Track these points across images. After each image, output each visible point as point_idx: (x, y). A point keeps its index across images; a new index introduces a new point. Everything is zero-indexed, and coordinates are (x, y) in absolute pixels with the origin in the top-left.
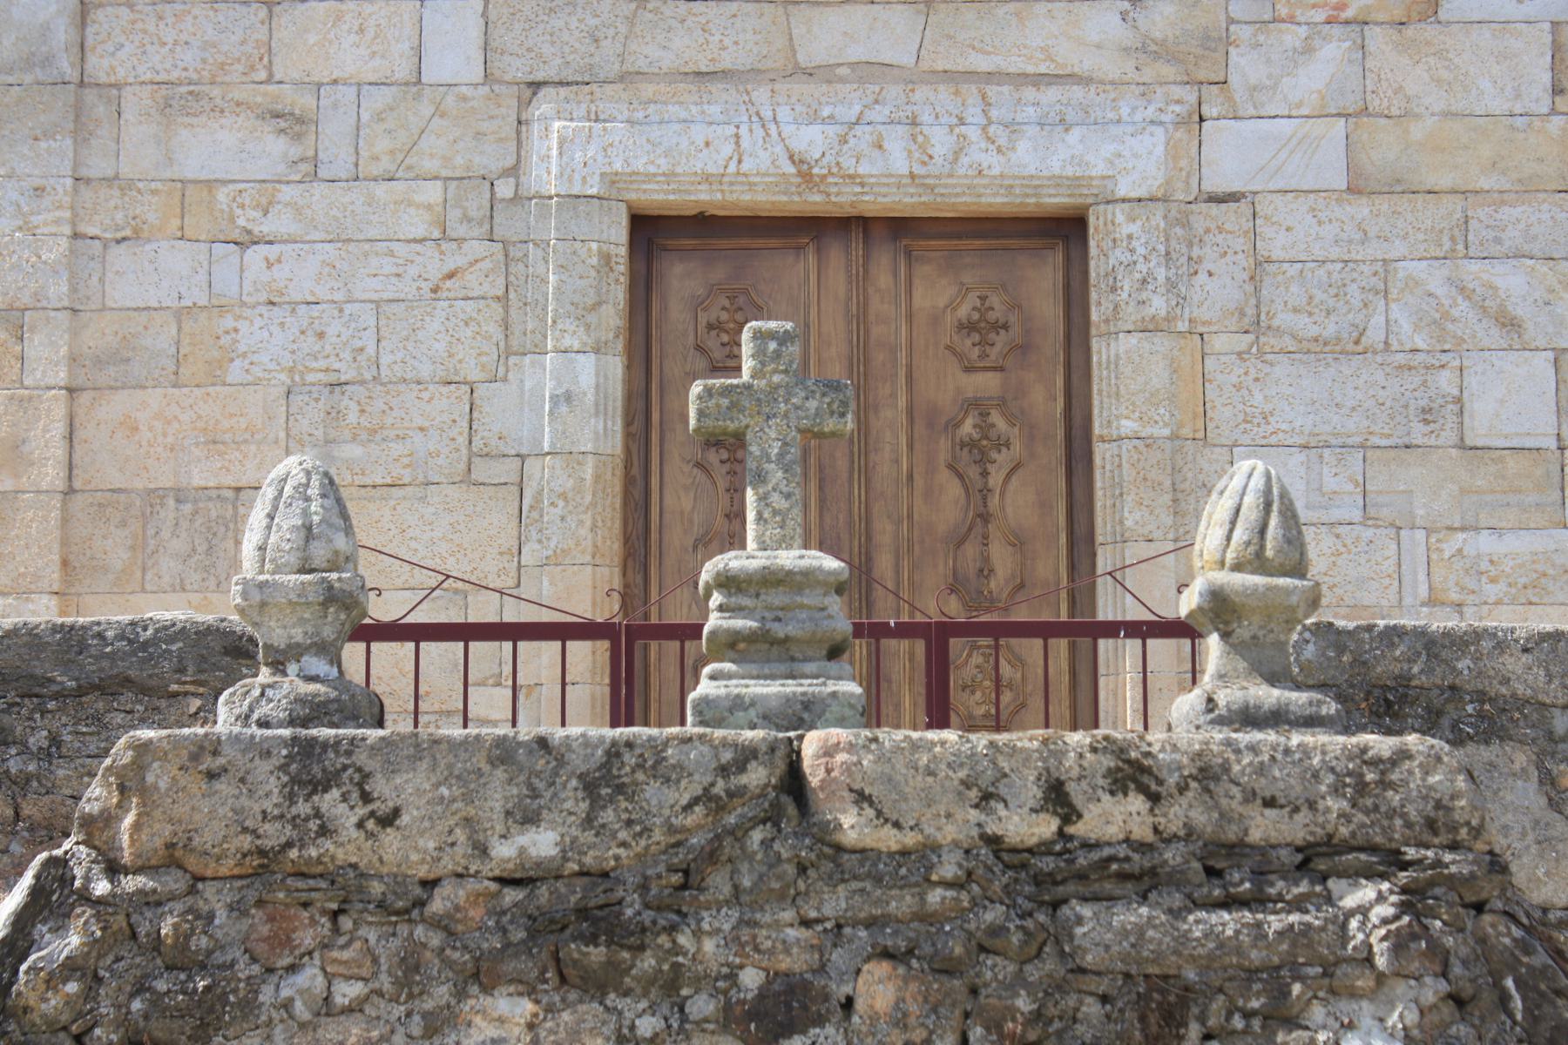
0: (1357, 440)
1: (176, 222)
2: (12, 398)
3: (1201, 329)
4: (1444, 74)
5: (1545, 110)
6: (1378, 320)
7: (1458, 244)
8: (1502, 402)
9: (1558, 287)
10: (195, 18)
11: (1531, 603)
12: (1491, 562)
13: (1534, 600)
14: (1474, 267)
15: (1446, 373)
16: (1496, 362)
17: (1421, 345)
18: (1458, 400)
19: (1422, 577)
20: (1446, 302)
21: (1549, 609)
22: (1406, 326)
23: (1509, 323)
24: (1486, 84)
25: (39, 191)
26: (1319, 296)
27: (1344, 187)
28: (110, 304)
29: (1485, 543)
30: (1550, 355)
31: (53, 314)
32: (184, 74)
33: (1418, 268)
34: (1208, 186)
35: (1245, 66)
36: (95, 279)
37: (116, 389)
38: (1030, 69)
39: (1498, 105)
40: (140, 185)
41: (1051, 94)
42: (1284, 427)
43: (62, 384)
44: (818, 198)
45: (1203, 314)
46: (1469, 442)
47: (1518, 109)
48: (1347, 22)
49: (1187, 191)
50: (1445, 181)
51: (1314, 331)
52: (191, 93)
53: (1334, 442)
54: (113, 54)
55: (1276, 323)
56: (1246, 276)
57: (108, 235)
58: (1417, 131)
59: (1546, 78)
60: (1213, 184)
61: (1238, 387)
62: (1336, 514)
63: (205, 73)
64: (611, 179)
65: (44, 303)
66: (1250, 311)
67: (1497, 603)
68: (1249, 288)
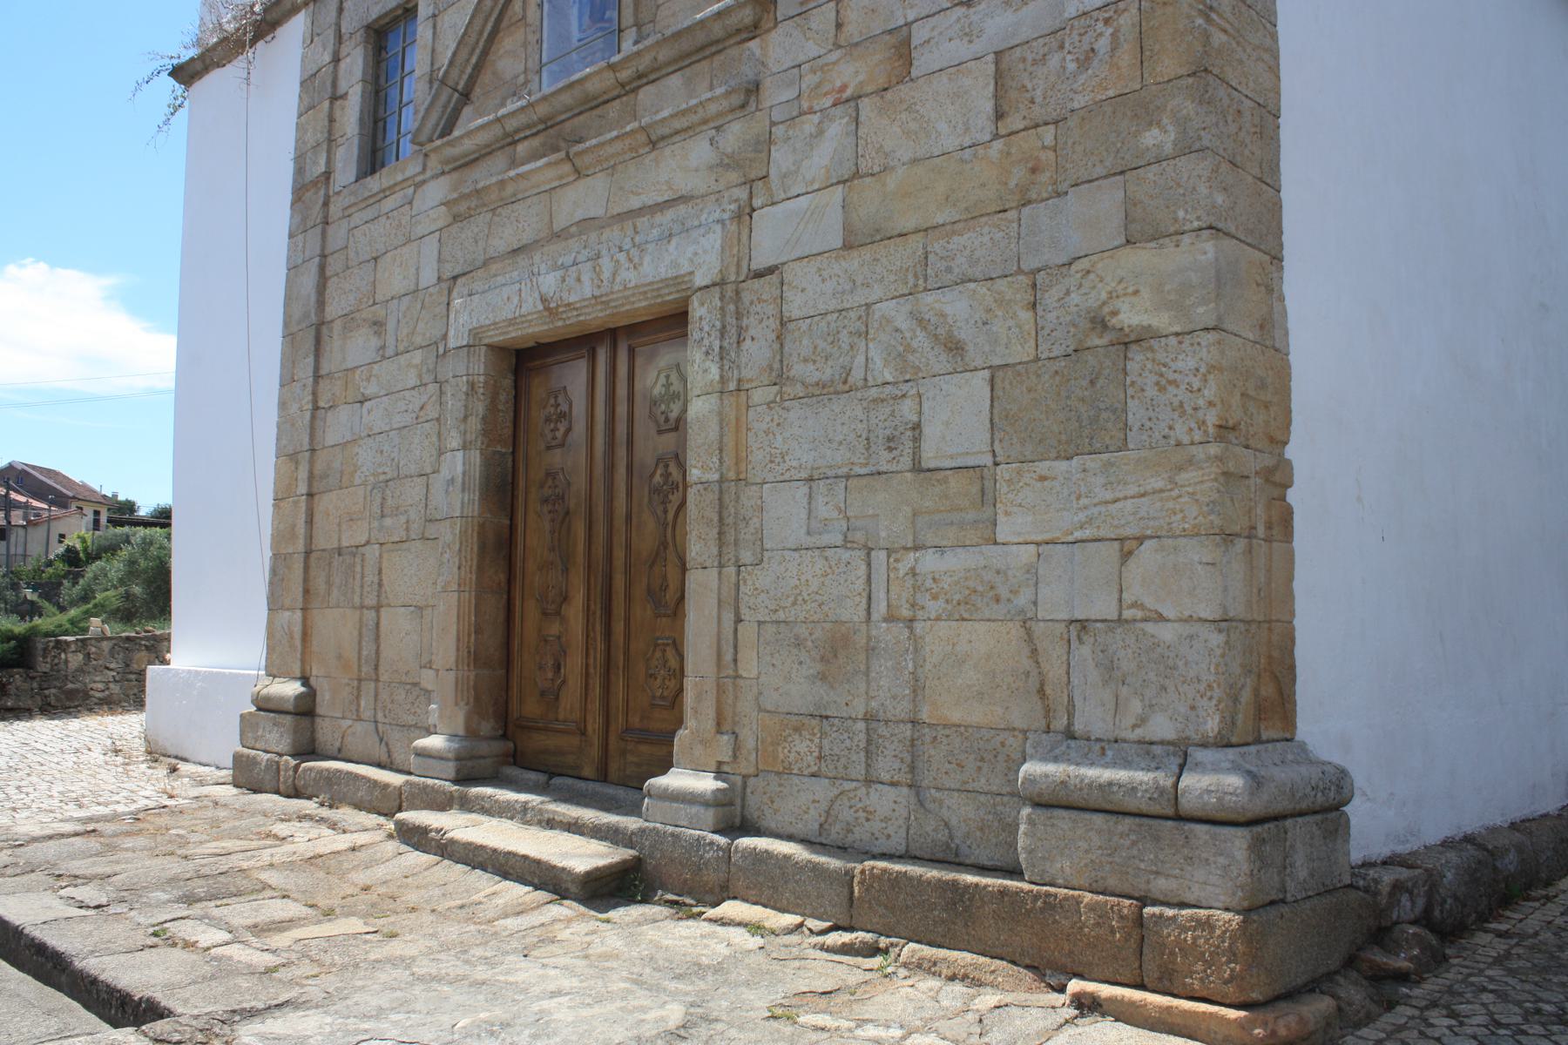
0: (845, 470)
3: (747, 386)
4: (913, 126)
5: (988, 137)
6: (861, 359)
7: (921, 279)
8: (947, 424)
9: (994, 306)
11: (964, 619)
12: (934, 579)
13: (966, 615)
14: (929, 298)
15: (908, 402)
16: (944, 387)
17: (891, 379)
18: (917, 427)
19: (882, 595)
20: (908, 335)
21: (976, 625)
22: (878, 362)
23: (955, 347)
24: (943, 127)
26: (821, 344)
27: (839, 244)
29: (929, 562)
30: (986, 374)
33: (887, 308)
34: (754, 267)
35: (781, 158)
38: (660, 199)
39: (950, 143)
41: (670, 214)
42: (794, 464)
44: (560, 323)
45: (747, 373)
46: (924, 465)
47: (967, 142)
48: (847, 101)
49: (738, 273)
50: (910, 225)
51: (816, 376)
53: (829, 473)
55: (792, 373)
56: (773, 336)
58: (892, 182)
59: (988, 106)
60: (759, 263)
61: (767, 433)
62: (826, 539)
64: (475, 333)
66: (776, 366)
67: (938, 619)
68: (776, 346)
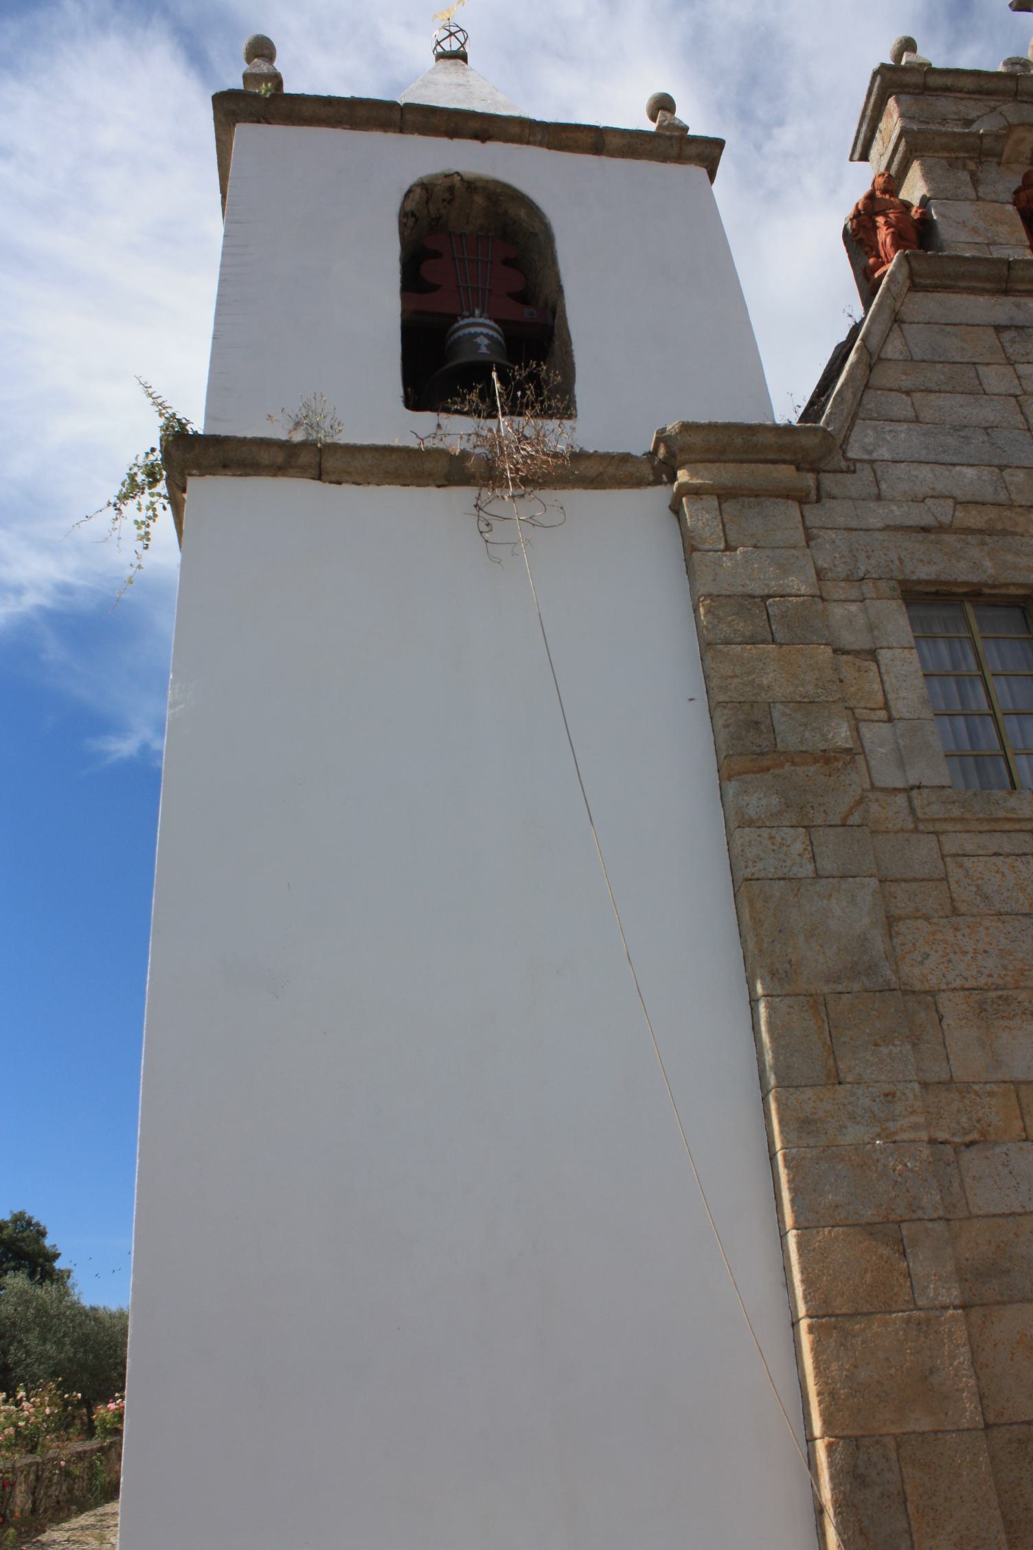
1: (1018, 1124)
2: (908, 1321)
10: (987, 928)
25: (890, 1096)
28: (975, 1211)
31: (930, 1225)
32: (990, 980)
36: (956, 1185)
37: (1004, 1303)
40: (976, 1087)
43: (957, 1302)
52: (1000, 997)
54: (922, 963)
57: (957, 1140)
63: (1008, 979)
65: (920, 1214)
